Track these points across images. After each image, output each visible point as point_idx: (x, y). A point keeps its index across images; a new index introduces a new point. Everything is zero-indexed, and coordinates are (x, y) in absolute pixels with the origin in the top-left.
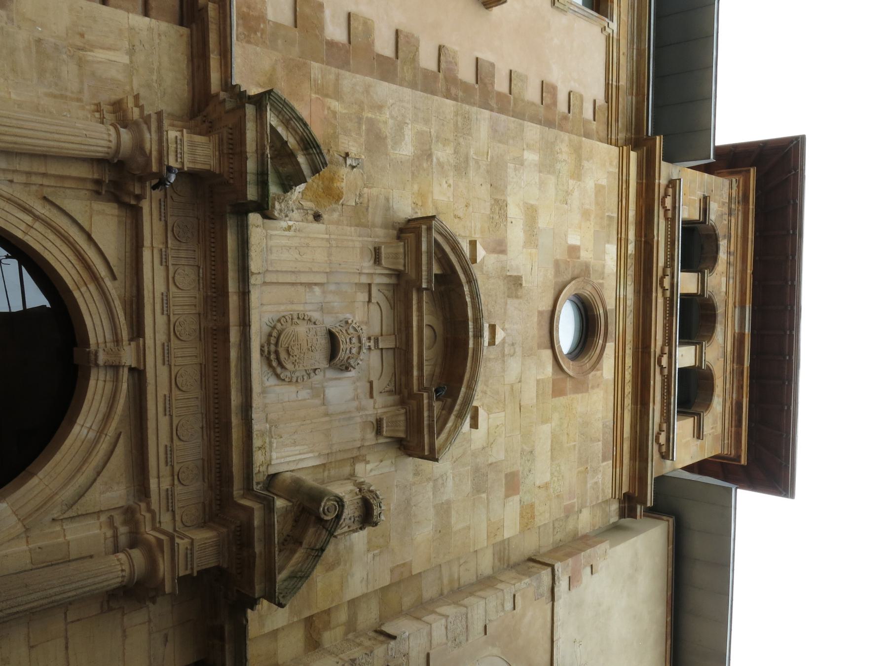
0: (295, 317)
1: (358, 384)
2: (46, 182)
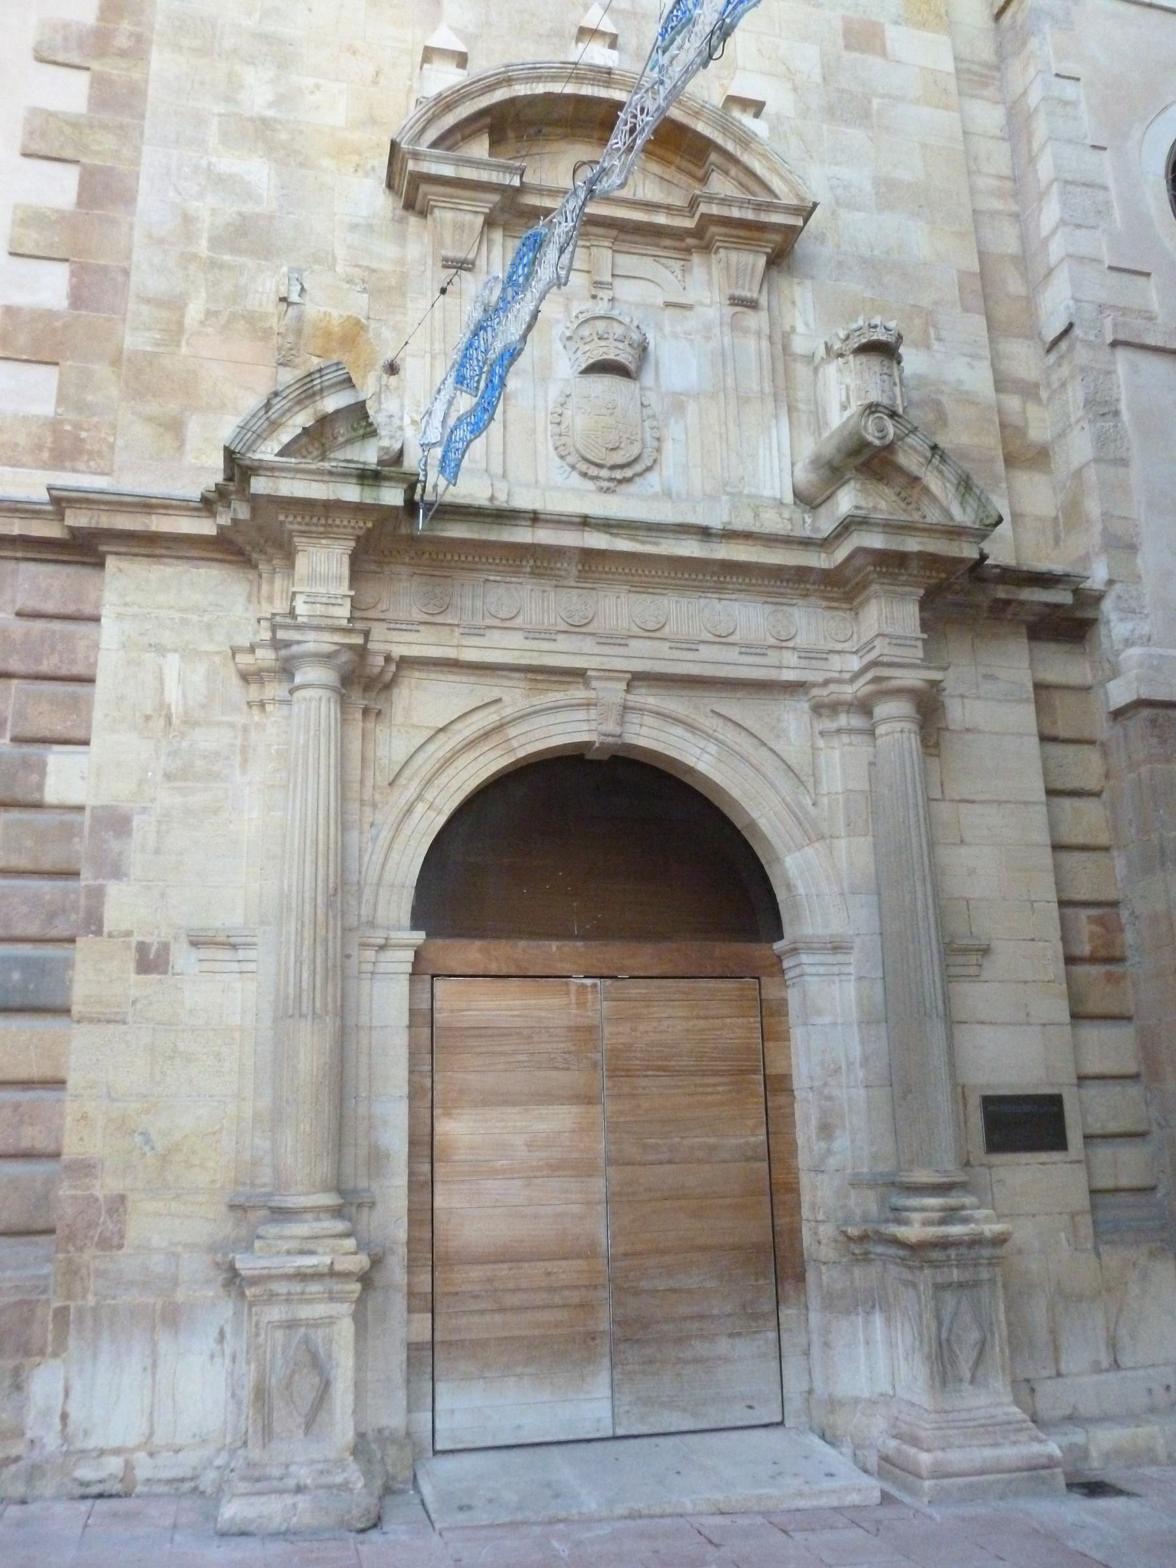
0: (557, 430)
2: (369, 783)
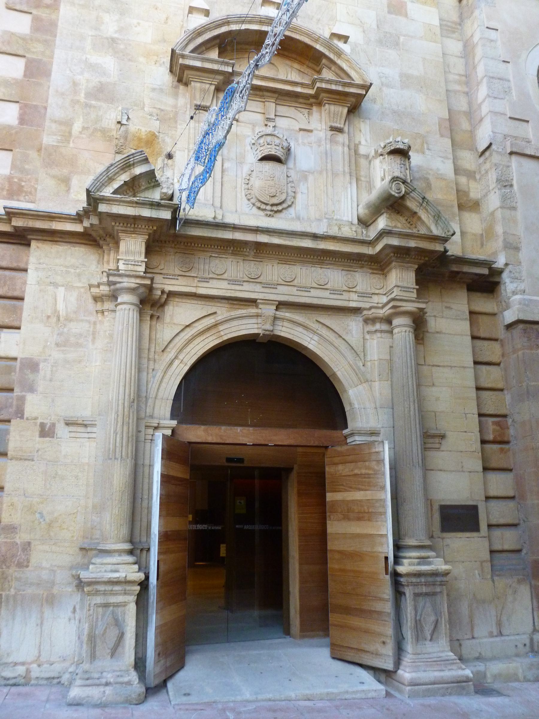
0: (247, 187)
1: (300, 141)
2: (153, 350)
